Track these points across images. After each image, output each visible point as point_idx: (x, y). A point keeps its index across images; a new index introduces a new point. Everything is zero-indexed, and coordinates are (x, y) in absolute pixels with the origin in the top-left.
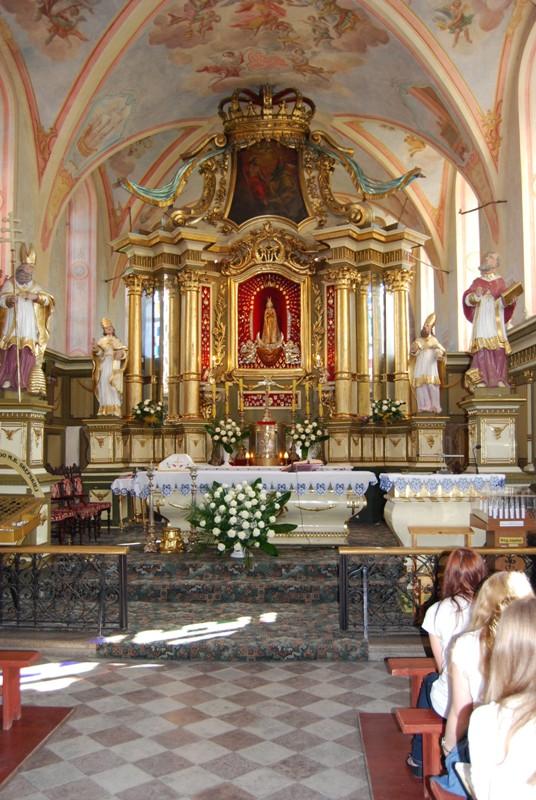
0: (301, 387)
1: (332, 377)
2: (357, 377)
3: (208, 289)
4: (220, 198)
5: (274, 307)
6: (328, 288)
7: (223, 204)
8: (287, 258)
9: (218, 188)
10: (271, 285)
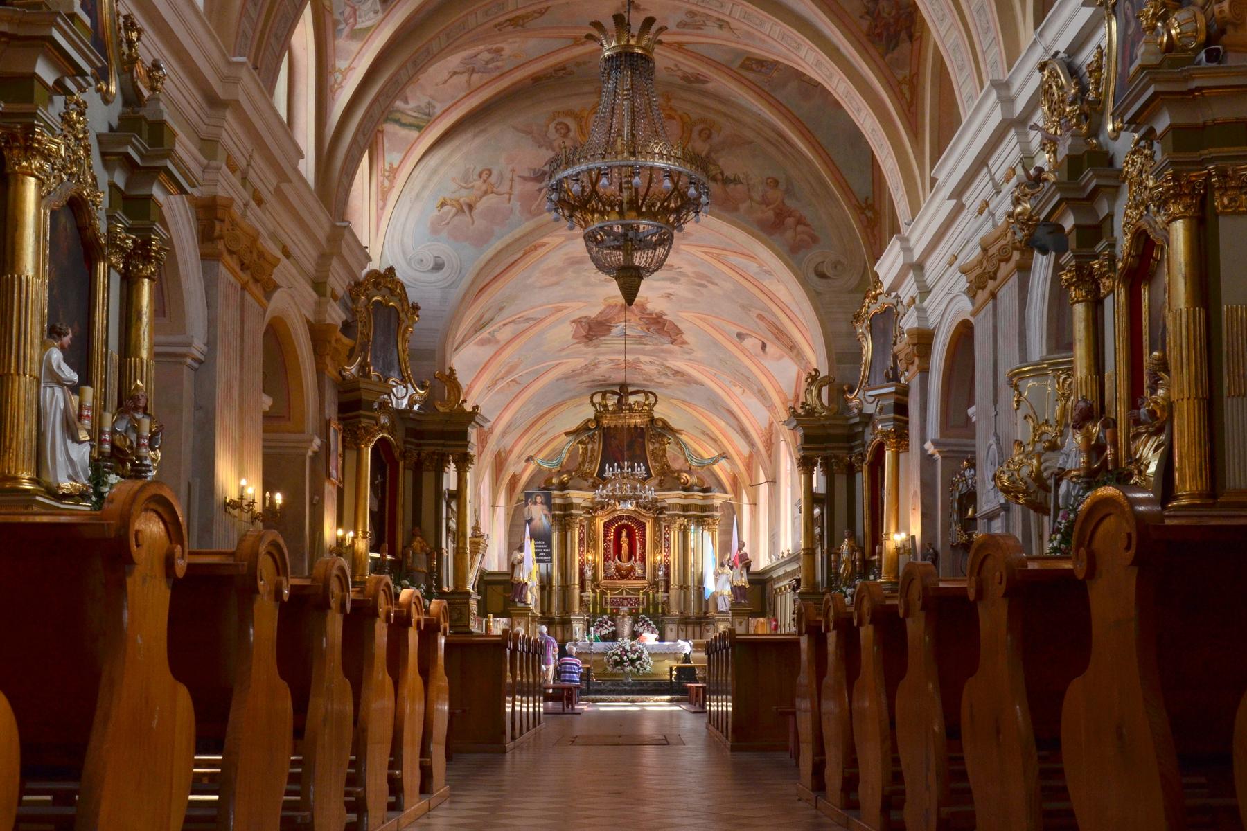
0: (646, 593)
1: (667, 590)
2: (684, 587)
3: (583, 526)
4: (591, 461)
6: (665, 527)
7: (593, 466)
9: (589, 454)
10: (626, 522)
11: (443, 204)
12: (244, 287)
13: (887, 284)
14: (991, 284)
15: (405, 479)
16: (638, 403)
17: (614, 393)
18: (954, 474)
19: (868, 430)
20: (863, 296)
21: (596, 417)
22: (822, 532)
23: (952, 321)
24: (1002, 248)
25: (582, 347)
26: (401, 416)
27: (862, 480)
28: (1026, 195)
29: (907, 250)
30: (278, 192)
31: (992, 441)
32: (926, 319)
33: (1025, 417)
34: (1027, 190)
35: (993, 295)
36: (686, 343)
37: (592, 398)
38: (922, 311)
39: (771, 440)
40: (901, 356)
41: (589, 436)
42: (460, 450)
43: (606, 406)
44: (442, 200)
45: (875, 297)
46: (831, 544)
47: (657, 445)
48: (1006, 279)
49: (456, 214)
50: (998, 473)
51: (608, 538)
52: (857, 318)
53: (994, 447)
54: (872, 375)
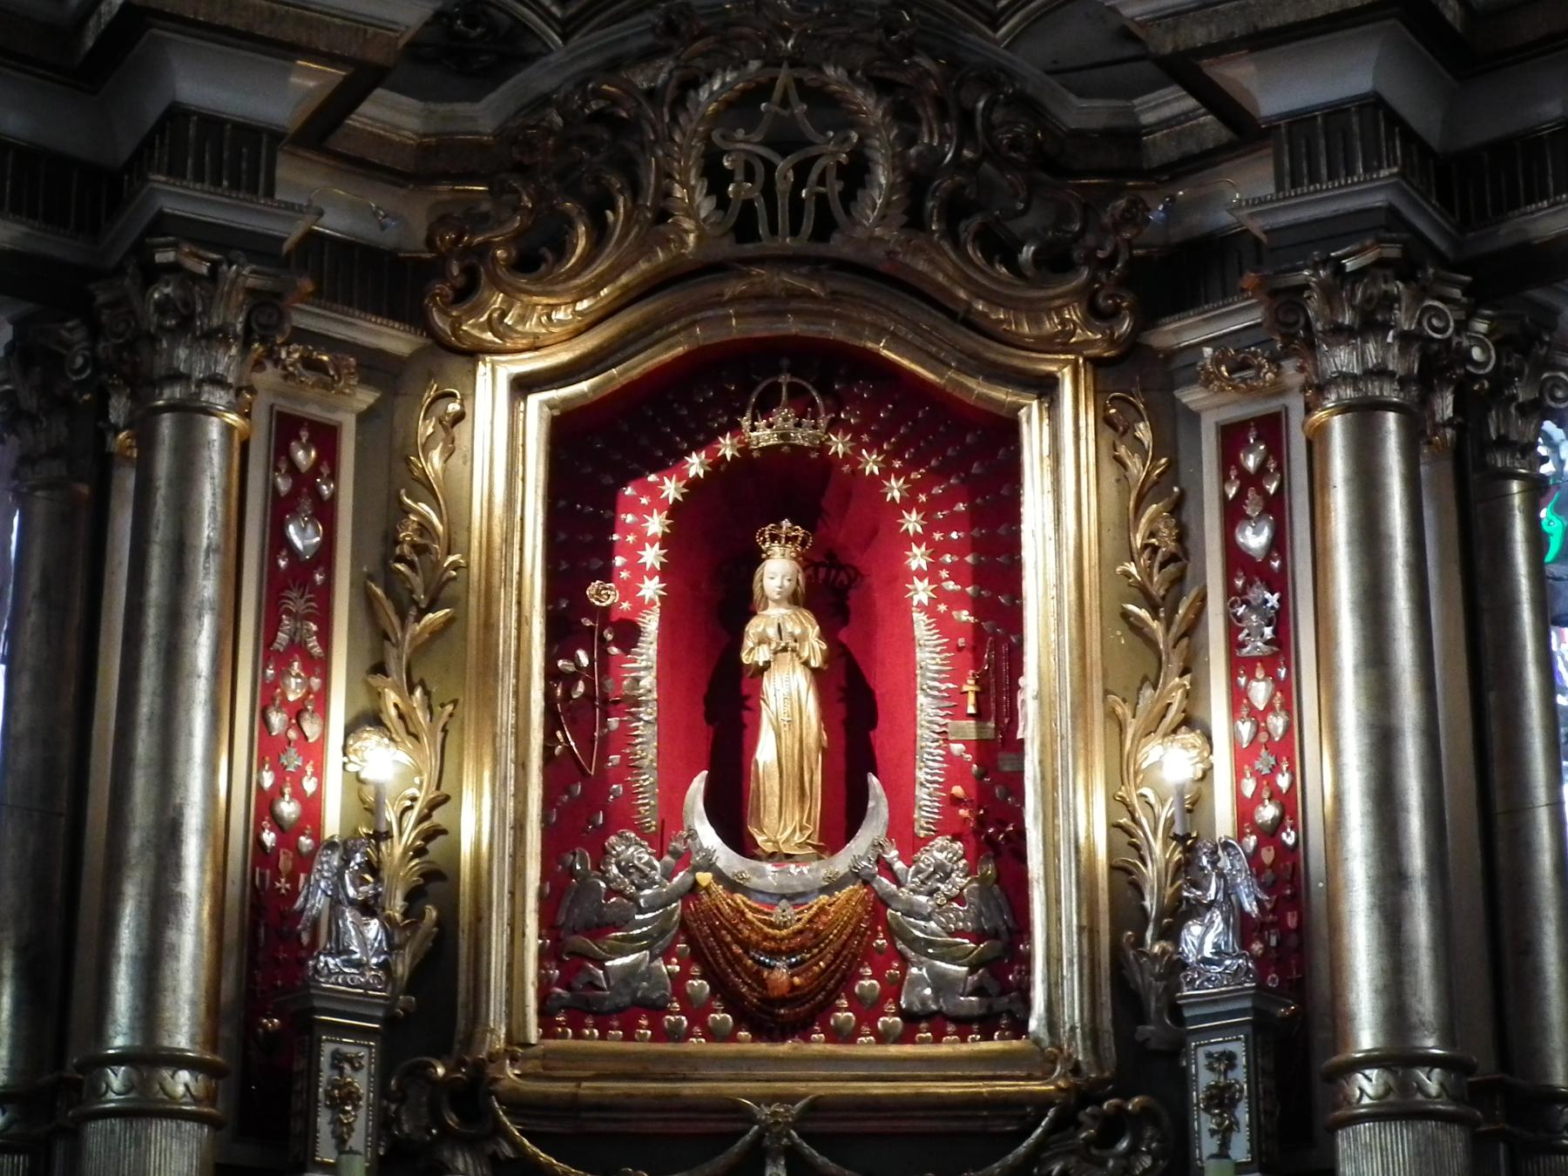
8: (915, 220)
51: (601, 594)
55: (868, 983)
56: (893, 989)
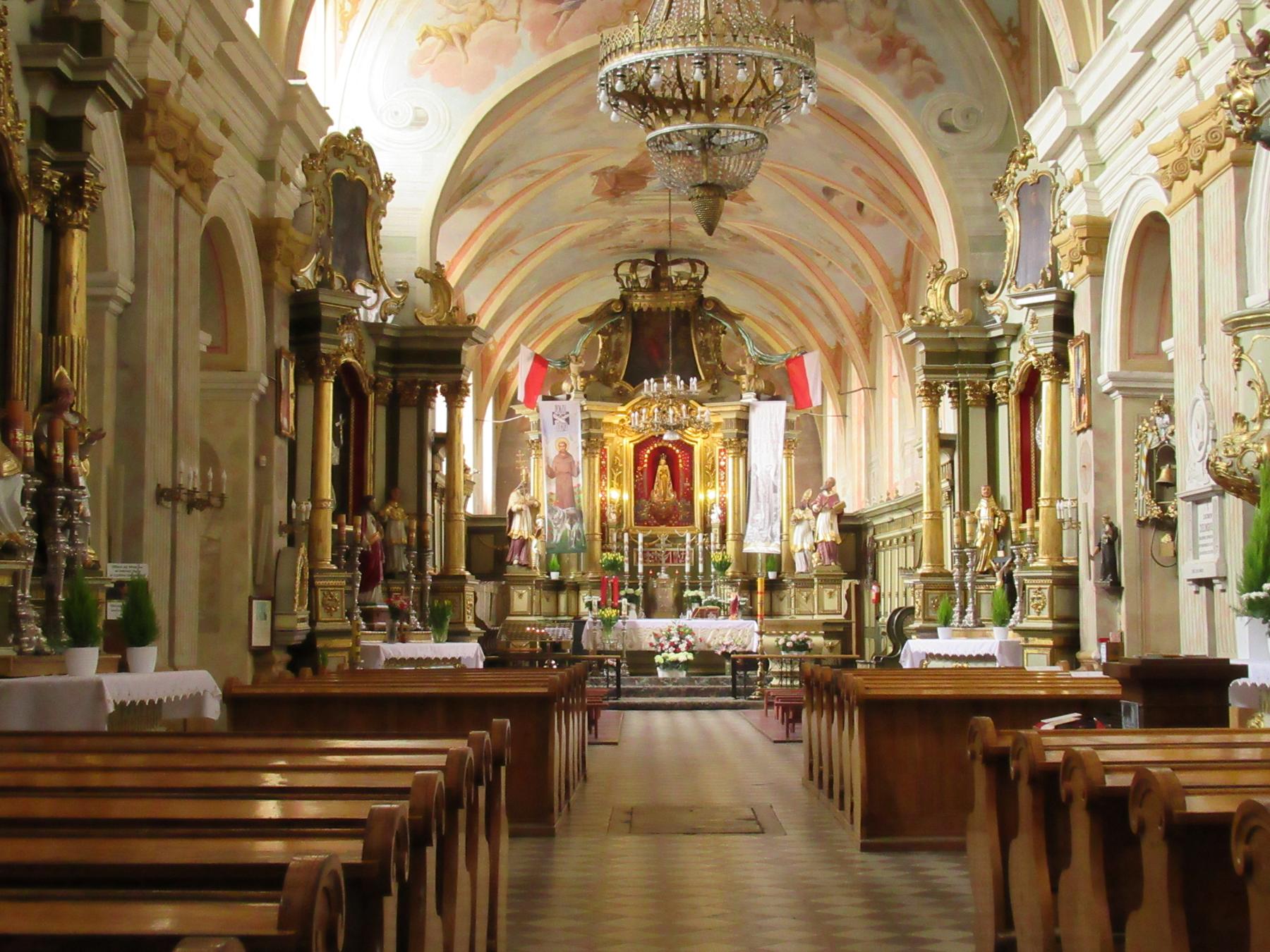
5: (667, 463)
6: (720, 451)
11: (425, 35)
12: (180, 192)
13: (1042, 151)
14: (1194, 178)
15: (377, 419)
16: (680, 276)
17: (649, 263)
18: (1140, 420)
19: (1016, 347)
20: (1007, 156)
21: (622, 296)
22: (953, 487)
23: (1137, 211)
24: (1211, 131)
25: (605, 205)
26: (374, 330)
27: (1006, 416)
28: (1247, 77)
29: (1071, 108)
30: (221, 55)
31: (1199, 393)
32: (1098, 202)
33: (1250, 383)
34: (1249, 71)
35: (1198, 193)
36: (751, 199)
37: (616, 269)
38: (1092, 191)
39: (868, 330)
40: (1063, 250)
41: (612, 323)
42: (451, 377)
43: (637, 281)
44: (424, 29)
45: (1024, 162)
46: (965, 504)
47: (709, 336)
48: (1216, 174)
49: (443, 48)
50: (1212, 460)
51: (639, 468)
52: (999, 188)
53: (1201, 403)
54: (1021, 269)
55: (673, 517)
56: (677, 518)
